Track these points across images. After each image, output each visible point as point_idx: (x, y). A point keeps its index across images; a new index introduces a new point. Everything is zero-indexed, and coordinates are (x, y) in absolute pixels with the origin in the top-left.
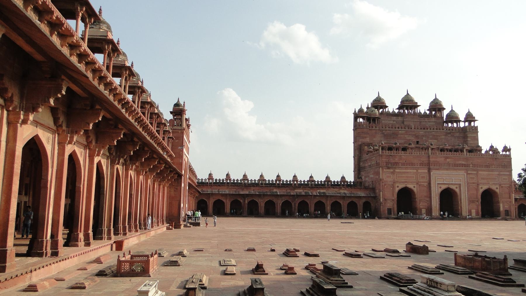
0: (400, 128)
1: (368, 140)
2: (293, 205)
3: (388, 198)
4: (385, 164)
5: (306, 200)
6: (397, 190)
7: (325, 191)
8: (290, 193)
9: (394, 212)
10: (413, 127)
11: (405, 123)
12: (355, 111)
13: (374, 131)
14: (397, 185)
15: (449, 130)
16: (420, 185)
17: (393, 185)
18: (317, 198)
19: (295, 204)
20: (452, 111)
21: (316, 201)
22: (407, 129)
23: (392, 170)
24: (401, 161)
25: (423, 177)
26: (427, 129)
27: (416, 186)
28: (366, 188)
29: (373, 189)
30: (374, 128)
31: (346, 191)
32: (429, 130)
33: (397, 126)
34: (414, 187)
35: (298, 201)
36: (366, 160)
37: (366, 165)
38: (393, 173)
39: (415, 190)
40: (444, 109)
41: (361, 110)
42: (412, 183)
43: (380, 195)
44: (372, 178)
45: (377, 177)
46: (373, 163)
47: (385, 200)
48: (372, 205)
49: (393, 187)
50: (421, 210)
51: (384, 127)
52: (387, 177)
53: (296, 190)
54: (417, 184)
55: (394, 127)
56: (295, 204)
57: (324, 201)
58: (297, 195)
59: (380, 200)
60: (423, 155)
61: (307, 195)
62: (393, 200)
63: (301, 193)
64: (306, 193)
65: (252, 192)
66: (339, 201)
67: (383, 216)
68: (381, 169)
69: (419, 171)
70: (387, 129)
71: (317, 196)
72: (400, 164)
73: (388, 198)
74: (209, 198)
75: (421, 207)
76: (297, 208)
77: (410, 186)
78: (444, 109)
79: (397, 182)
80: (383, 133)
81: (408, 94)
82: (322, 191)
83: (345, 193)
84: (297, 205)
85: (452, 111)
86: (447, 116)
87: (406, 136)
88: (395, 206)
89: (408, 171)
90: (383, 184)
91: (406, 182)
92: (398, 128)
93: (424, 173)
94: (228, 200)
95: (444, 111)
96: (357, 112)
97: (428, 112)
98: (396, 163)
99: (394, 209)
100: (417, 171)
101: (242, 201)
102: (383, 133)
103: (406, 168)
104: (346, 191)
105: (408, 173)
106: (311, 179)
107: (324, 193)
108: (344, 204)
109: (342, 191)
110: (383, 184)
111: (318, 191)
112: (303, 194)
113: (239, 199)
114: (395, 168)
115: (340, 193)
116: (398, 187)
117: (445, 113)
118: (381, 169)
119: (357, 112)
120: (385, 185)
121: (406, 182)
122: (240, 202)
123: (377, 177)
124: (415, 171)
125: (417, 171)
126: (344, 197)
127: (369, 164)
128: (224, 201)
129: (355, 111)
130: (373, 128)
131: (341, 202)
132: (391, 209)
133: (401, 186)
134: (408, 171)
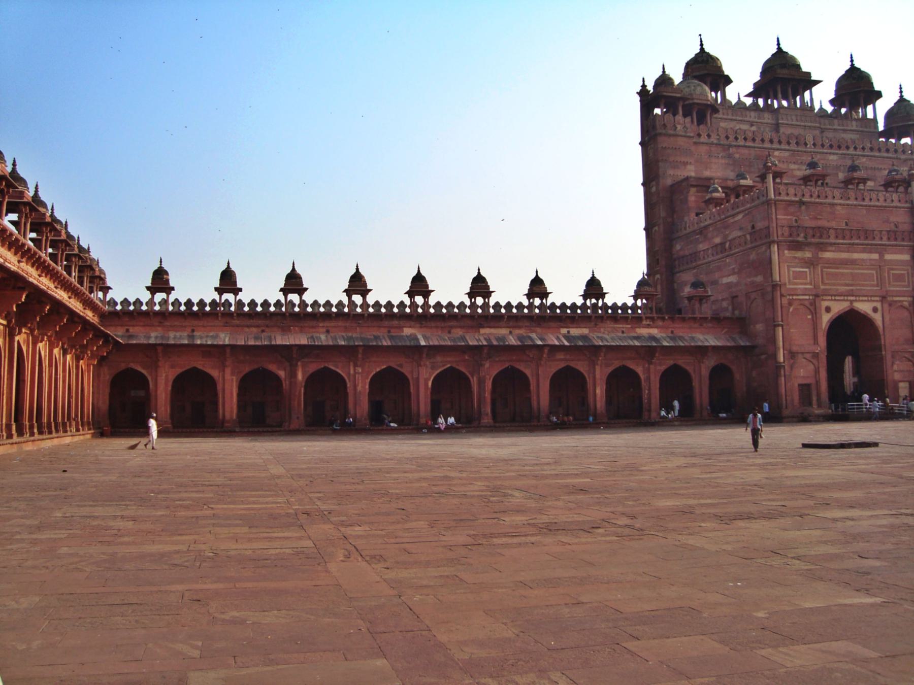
0: (776, 140)
1: (690, 171)
2: (474, 381)
3: (799, 350)
4: (786, 231)
5: (521, 367)
6: (826, 319)
7: (585, 331)
8: (463, 338)
9: (818, 395)
10: (810, 140)
11: (782, 130)
12: (644, 86)
13: (703, 149)
14: (825, 304)
15: (904, 152)
16: (890, 305)
17: (813, 303)
18: (560, 356)
19: (481, 382)
20: (902, 101)
21: (554, 367)
22: (793, 147)
23: (808, 255)
24: (833, 224)
25: (898, 278)
26: (848, 148)
27: (879, 305)
28: (717, 320)
29: (741, 324)
30: (704, 139)
31: (654, 331)
32: (851, 151)
33: (767, 137)
34: (875, 310)
35: (491, 370)
36: (702, 231)
37: (701, 247)
38: (811, 263)
39: (877, 318)
40: (879, 95)
41: (664, 80)
42: (869, 297)
43: (773, 340)
44: (729, 285)
45: (759, 279)
46: (736, 233)
47: (792, 355)
48: (737, 376)
49: (813, 309)
50: (896, 383)
51: (732, 138)
52: (797, 275)
53: (482, 331)
54: (883, 298)
55: (758, 139)
56: (481, 382)
57: (581, 366)
58: (491, 347)
59: (774, 356)
60: (896, 204)
61: (523, 349)
62: (816, 355)
63: (503, 339)
64: (520, 338)
65: (323, 339)
66: (631, 365)
67: (786, 412)
68: (775, 248)
69: (888, 257)
70: (741, 142)
71: (562, 348)
72: (832, 232)
73: (799, 350)
74: (154, 367)
75: (897, 376)
76: (488, 395)
77: (865, 307)
78: (879, 95)
79: (826, 293)
80: (730, 156)
81: (779, 49)
82: (575, 332)
83: (652, 338)
84: (489, 385)
85: (902, 101)
86: (889, 115)
87: (793, 166)
88: (823, 374)
89: (856, 256)
90: (785, 301)
91: (850, 293)
92: (771, 141)
93: (902, 262)
94: (228, 371)
95: (879, 103)
96: (650, 87)
97: (829, 109)
98: (821, 231)
99: (818, 382)
100: (881, 256)
101: (282, 374)
102: (730, 156)
103: (851, 248)
104: (654, 331)
105: (853, 262)
106: (536, 289)
107: (584, 337)
108: (650, 376)
109: (644, 332)
110: (785, 301)
111: (564, 331)
112: (512, 341)
113: (272, 367)
114: (822, 247)
115: (637, 338)
116: (828, 309)
117: (883, 106)
118: (775, 248)
119: (650, 87)
120: (790, 304)
121: (850, 293)
122: (278, 378)
123: (759, 279)
124: (875, 256)
125: (881, 256)
126: (649, 352)
127: (717, 240)
128: (215, 373)
129: (644, 86)
130: (702, 140)
131: (639, 370)
132: (808, 386)
133: (838, 307)
134: (856, 256)
